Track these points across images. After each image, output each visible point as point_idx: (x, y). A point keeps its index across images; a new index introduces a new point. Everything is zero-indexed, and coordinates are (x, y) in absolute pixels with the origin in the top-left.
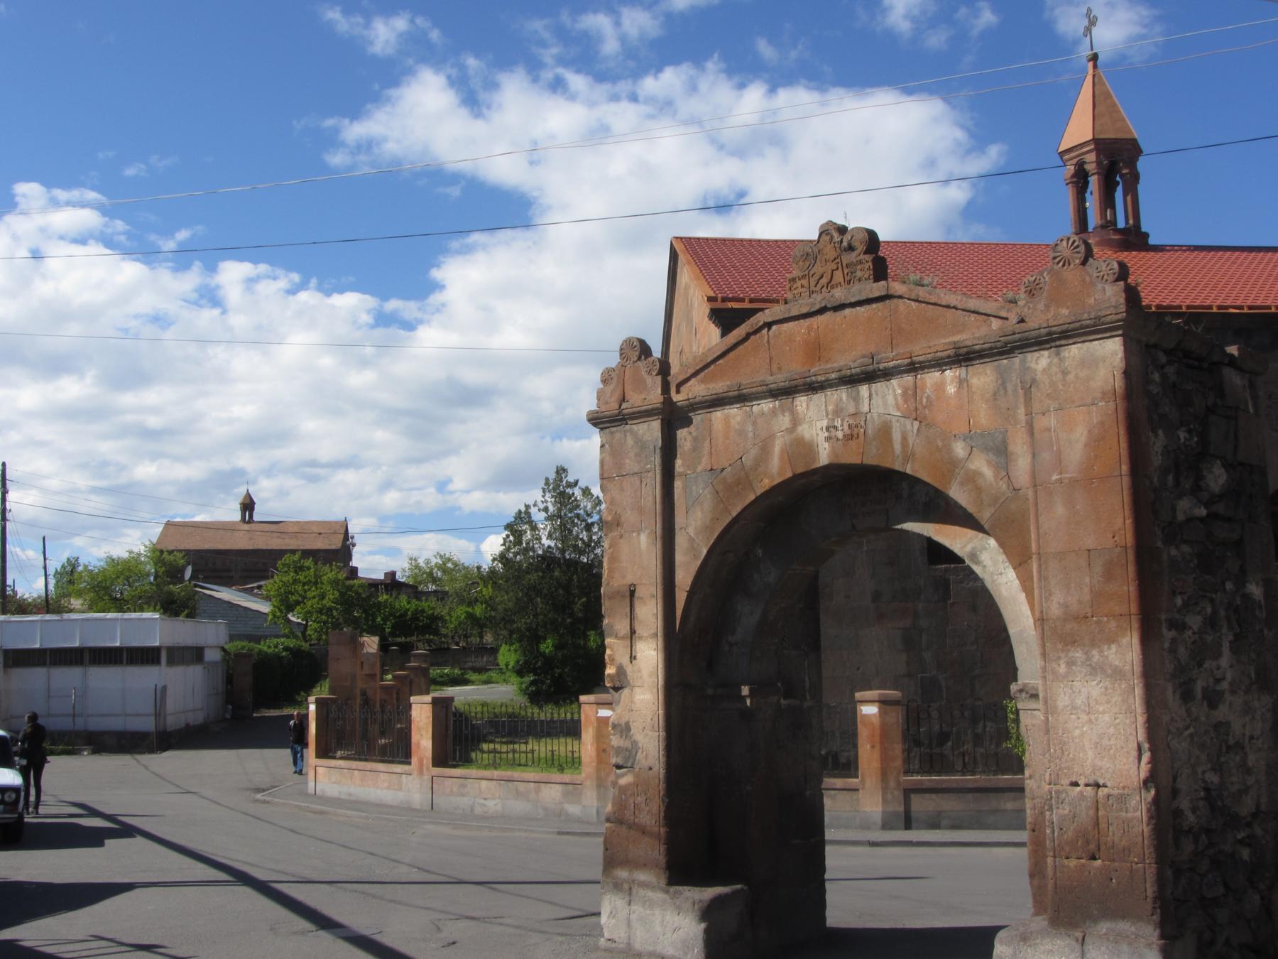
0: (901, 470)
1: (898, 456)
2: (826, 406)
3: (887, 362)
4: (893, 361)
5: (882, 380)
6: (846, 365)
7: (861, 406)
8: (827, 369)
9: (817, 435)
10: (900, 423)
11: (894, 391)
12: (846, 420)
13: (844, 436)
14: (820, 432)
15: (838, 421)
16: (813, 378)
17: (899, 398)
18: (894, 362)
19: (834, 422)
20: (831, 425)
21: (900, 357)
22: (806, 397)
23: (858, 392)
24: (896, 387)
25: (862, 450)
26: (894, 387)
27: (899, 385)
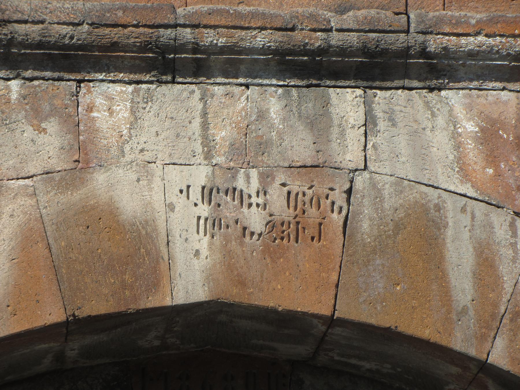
0: (472, 352)
1: (464, 310)
2: (205, 126)
3: (458, 35)
4: (477, 34)
5: (415, 83)
6: (312, 17)
7: (334, 145)
8: (239, 15)
9: (171, 207)
10: (473, 217)
11: (452, 120)
12: (280, 178)
13: (271, 225)
14: (180, 202)
15: (248, 177)
16: (187, 34)
17: (470, 145)
18: (481, 38)
19: (234, 177)
20: (220, 182)
21: (498, 28)
22: (130, 88)
23: (327, 103)
24: (460, 112)
25: (334, 277)
26: (451, 111)
27: (469, 108)
